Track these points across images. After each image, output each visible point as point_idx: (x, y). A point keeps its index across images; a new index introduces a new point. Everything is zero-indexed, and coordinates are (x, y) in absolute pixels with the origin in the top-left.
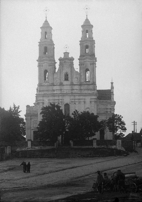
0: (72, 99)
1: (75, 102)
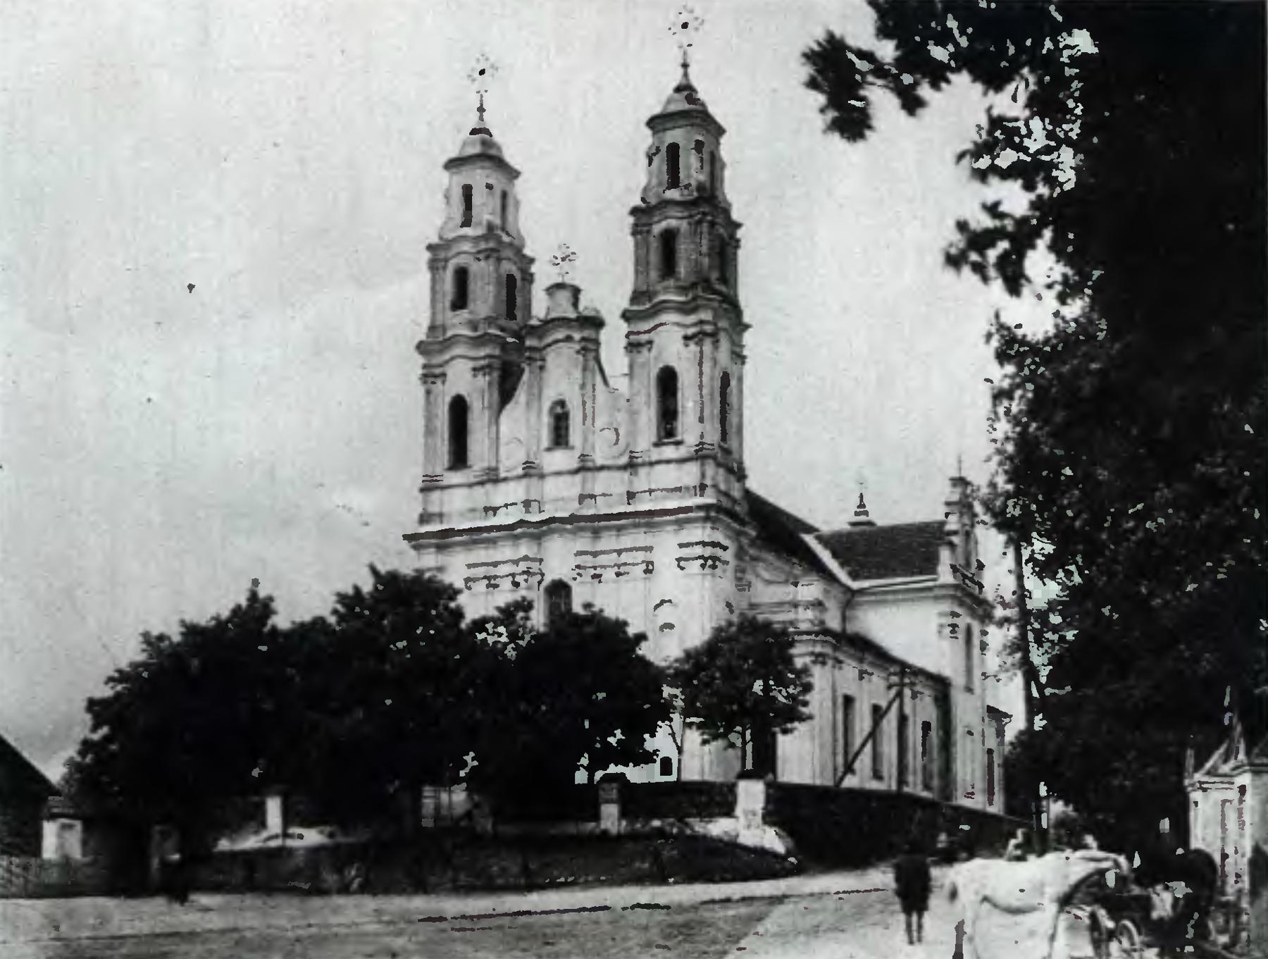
1: (598, 571)
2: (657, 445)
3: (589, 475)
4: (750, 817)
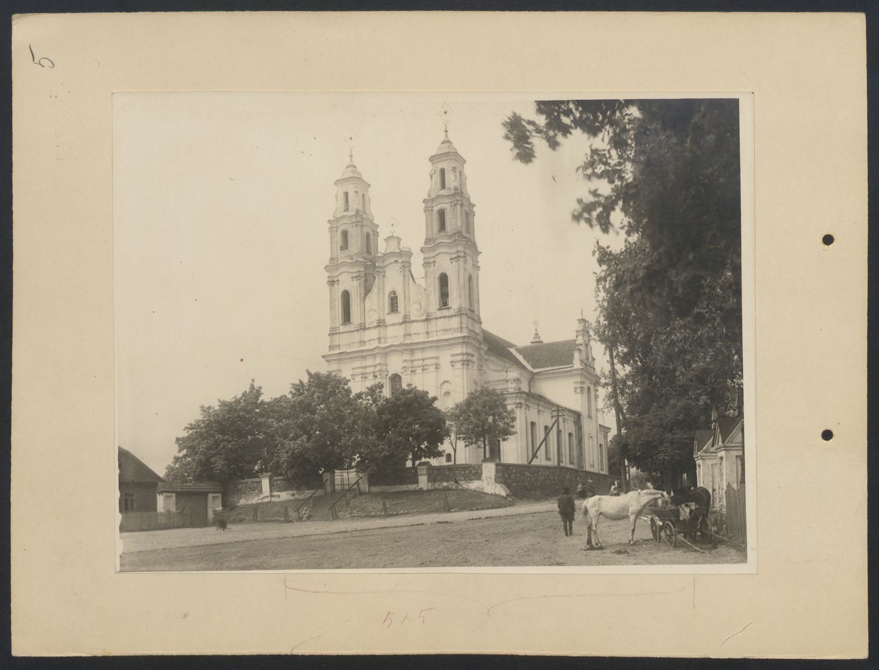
0: (405, 361)
1: (413, 369)
2: (439, 310)
3: (408, 325)
4: (489, 480)
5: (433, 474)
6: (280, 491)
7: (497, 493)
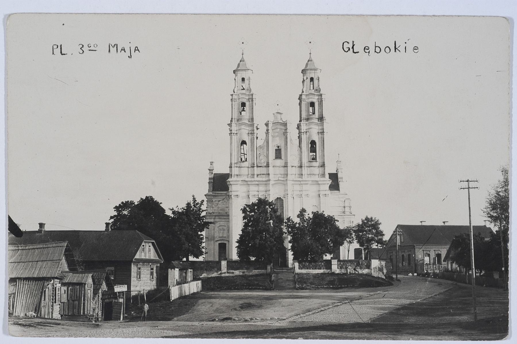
4: (375, 269)
5: (341, 264)
6: (235, 270)
7: (380, 276)
